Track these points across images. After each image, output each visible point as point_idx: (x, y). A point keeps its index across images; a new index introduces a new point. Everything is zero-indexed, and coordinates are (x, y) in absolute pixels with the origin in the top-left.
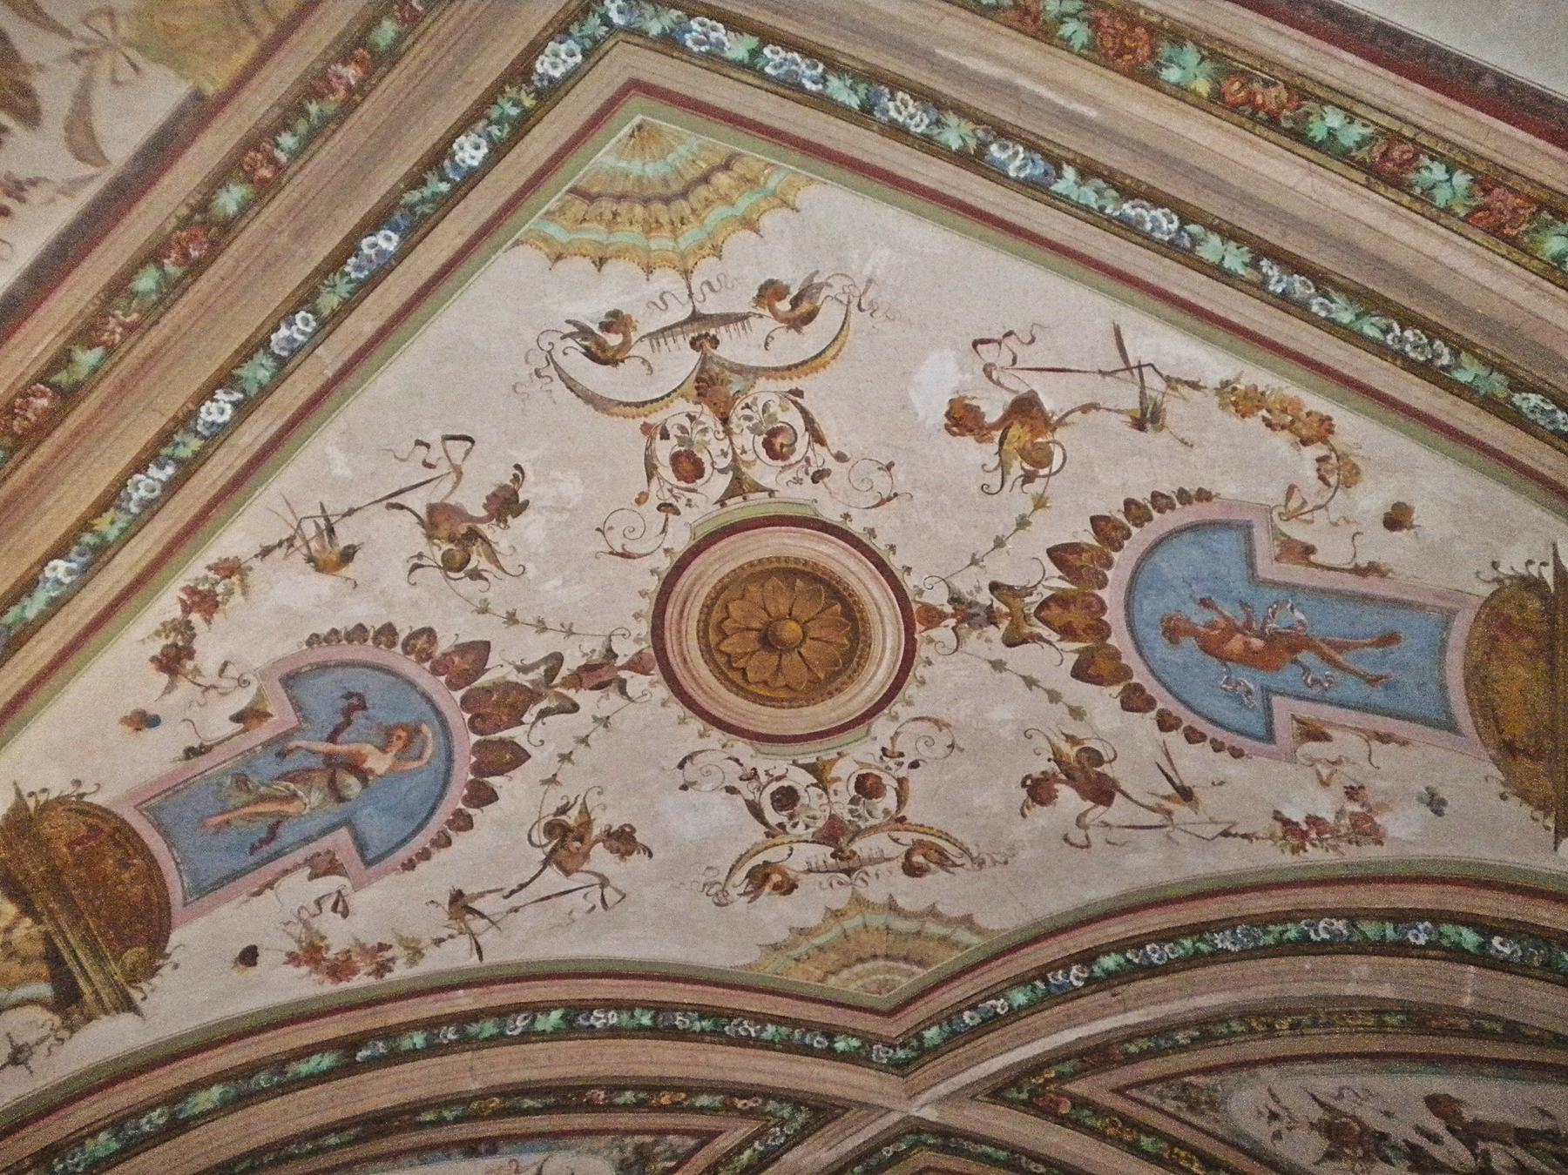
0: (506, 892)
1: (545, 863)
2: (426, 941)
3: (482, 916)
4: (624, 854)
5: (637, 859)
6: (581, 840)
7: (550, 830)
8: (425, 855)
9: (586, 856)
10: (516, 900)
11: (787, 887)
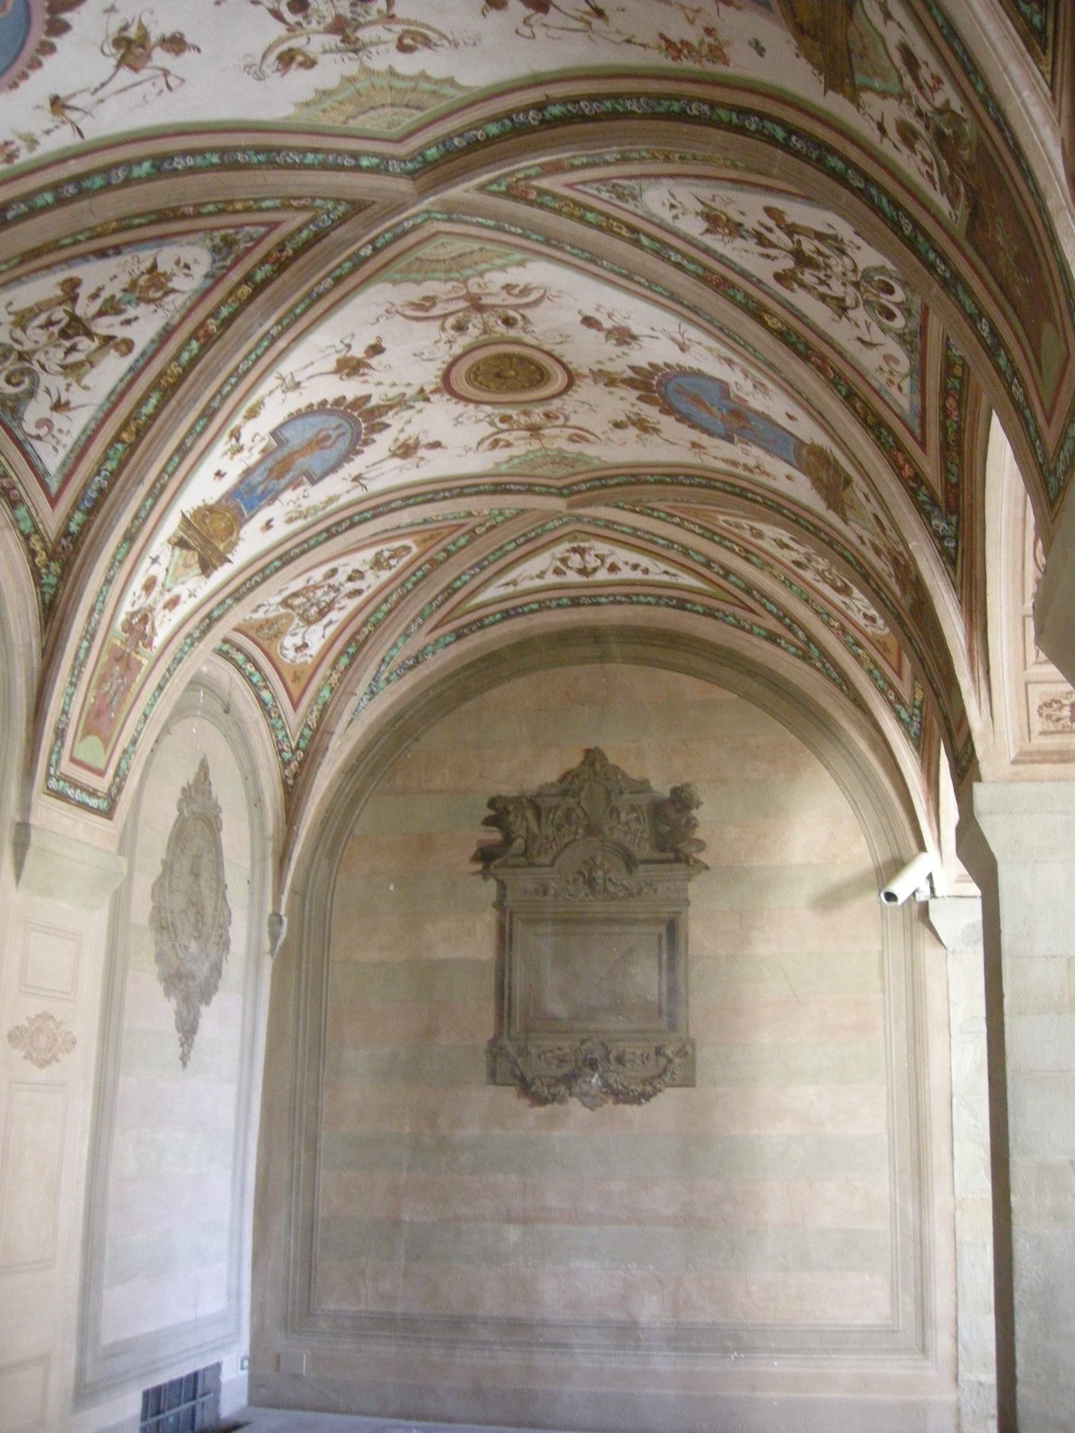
0: (92, 90)
1: (118, 66)
2: (38, 133)
3: (76, 109)
4: (178, 52)
5: (189, 55)
6: (143, 46)
7: (117, 43)
8: (24, 76)
9: (149, 57)
10: (100, 94)
11: (310, 63)
